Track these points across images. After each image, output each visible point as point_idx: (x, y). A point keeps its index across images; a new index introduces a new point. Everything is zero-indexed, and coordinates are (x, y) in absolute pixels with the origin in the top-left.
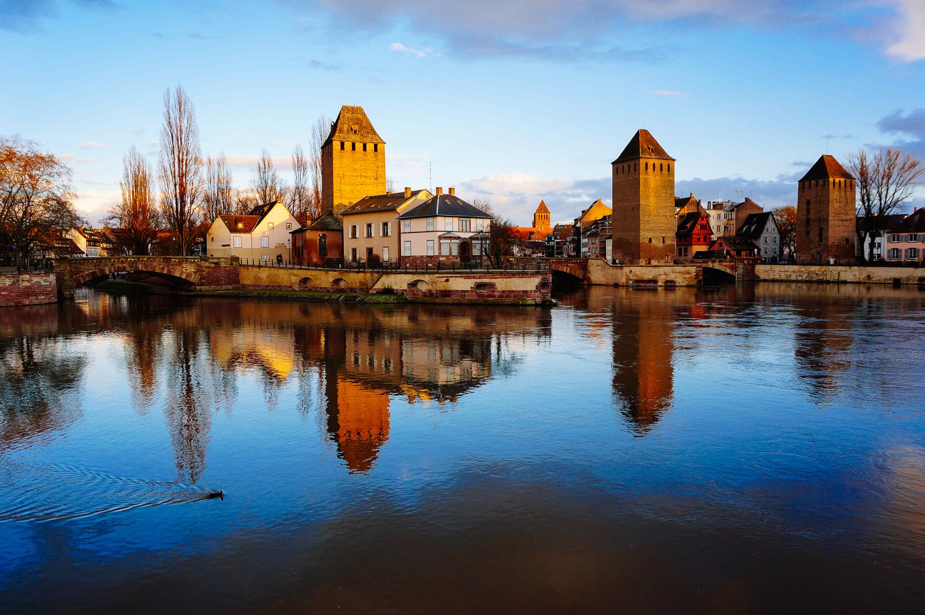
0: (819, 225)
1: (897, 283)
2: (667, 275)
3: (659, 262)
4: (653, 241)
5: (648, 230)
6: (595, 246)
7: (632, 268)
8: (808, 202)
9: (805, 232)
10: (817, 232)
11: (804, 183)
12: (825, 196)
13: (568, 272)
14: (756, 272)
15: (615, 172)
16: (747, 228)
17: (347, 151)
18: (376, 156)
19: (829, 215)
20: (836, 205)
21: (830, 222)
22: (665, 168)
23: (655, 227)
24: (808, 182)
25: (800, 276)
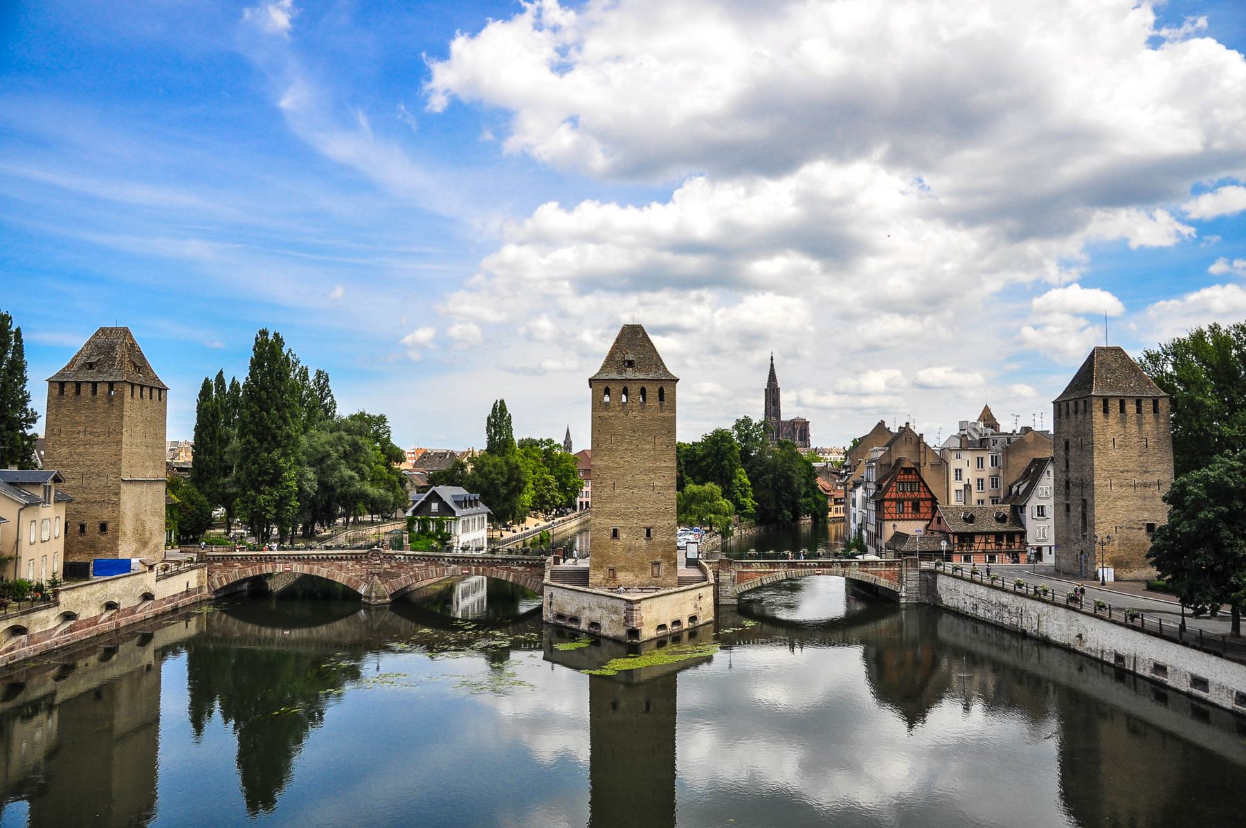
0: (1082, 495)
4: (623, 535)
9: (1064, 506)
10: (1080, 509)
12: (1088, 435)
14: (938, 589)
17: (67, 396)
18: (110, 400)
19: (1093, 475)
20: (1115, 454)
21: (1097, 491)
23: (627, 508)
25: (988, 611)
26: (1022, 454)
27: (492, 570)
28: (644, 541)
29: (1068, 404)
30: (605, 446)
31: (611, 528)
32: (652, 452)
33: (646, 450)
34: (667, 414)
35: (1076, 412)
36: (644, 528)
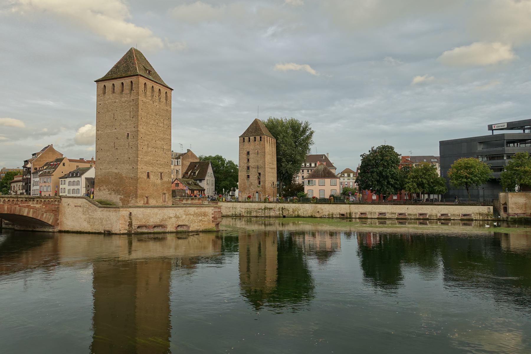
0: (258, 171)
1: (343, 217)
2: (178, 217)
3: (157, 202)
4: (151, 176)
5: (147, 163)
6: (47, 184)
7: (131, 210)
8: (248, 153)
9: (246, 177)
10: (256, 176)
11: (244, 139)
13: (31, 215)
15: (102, 92)
16: (191, 173)
22: (163, 95)
23: (153, 160)
24: (248, 138)
26: (187, 160)
27: (15, 208)
28: (160, 181)
29: (249, 138)
30: (144, 120)
31: (147, 172)
32: (163, 129)
33: (160, 126)
34: (168, 108)
35: (255, 141)
36: (160, 172)
